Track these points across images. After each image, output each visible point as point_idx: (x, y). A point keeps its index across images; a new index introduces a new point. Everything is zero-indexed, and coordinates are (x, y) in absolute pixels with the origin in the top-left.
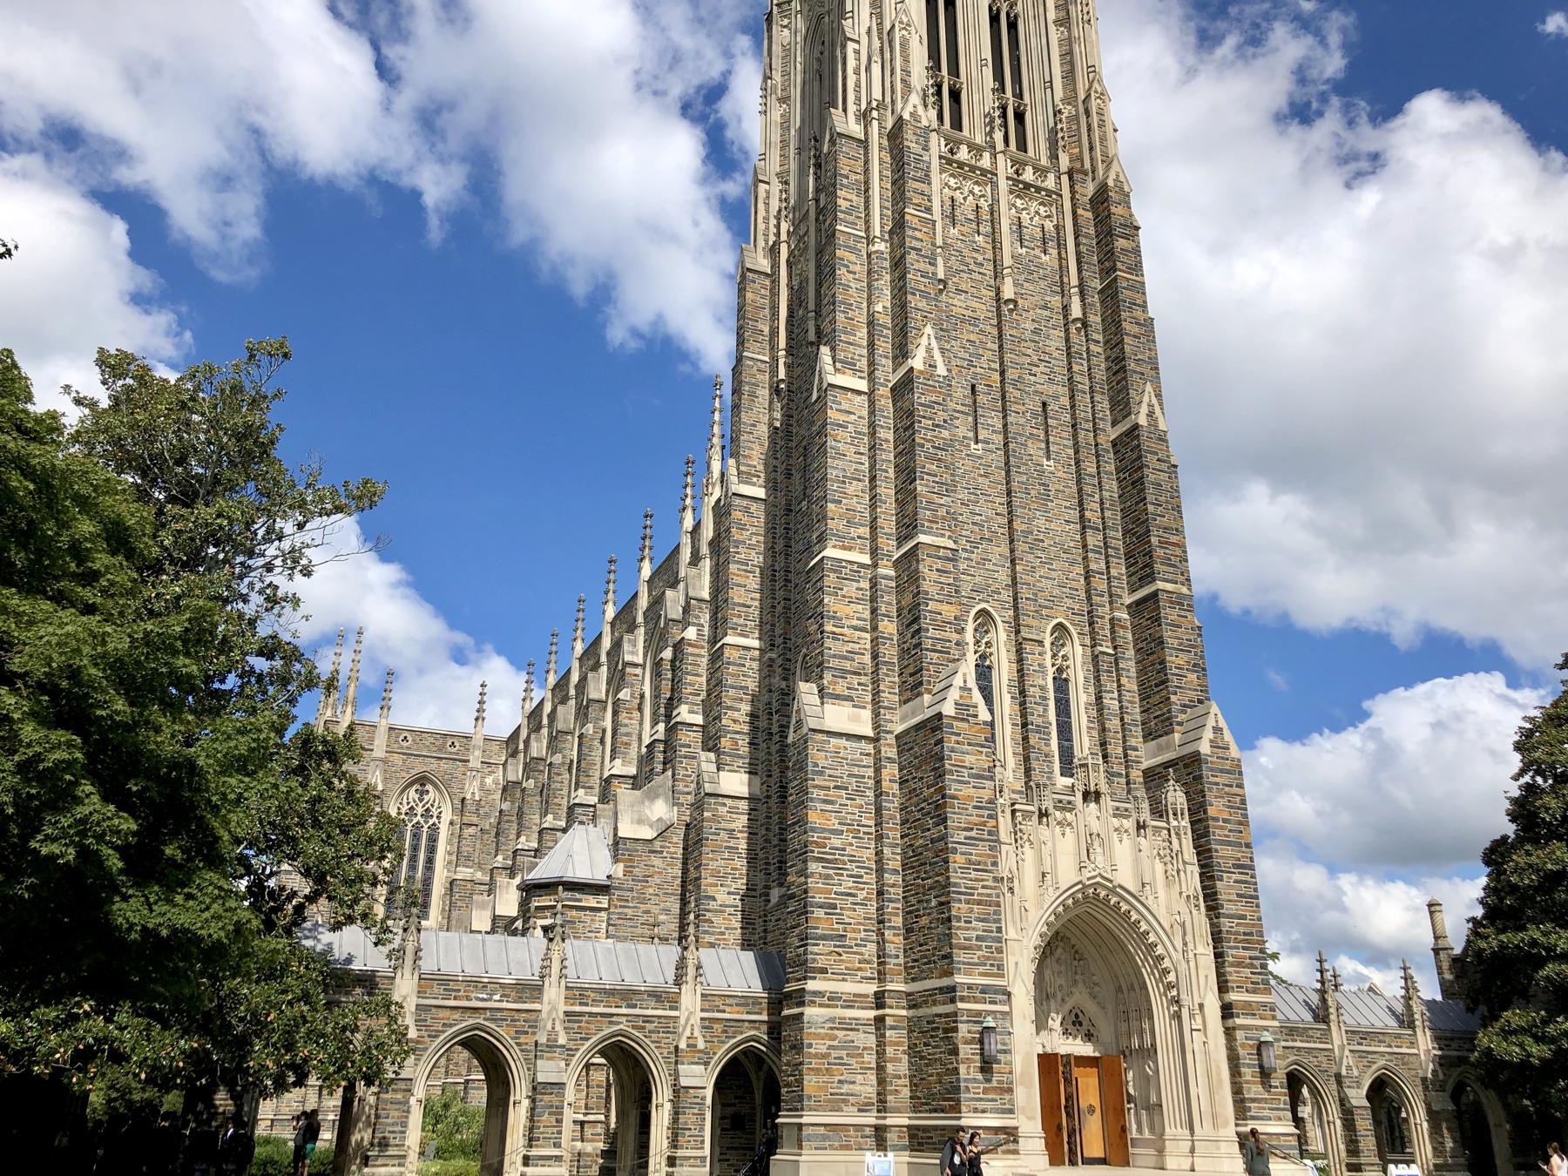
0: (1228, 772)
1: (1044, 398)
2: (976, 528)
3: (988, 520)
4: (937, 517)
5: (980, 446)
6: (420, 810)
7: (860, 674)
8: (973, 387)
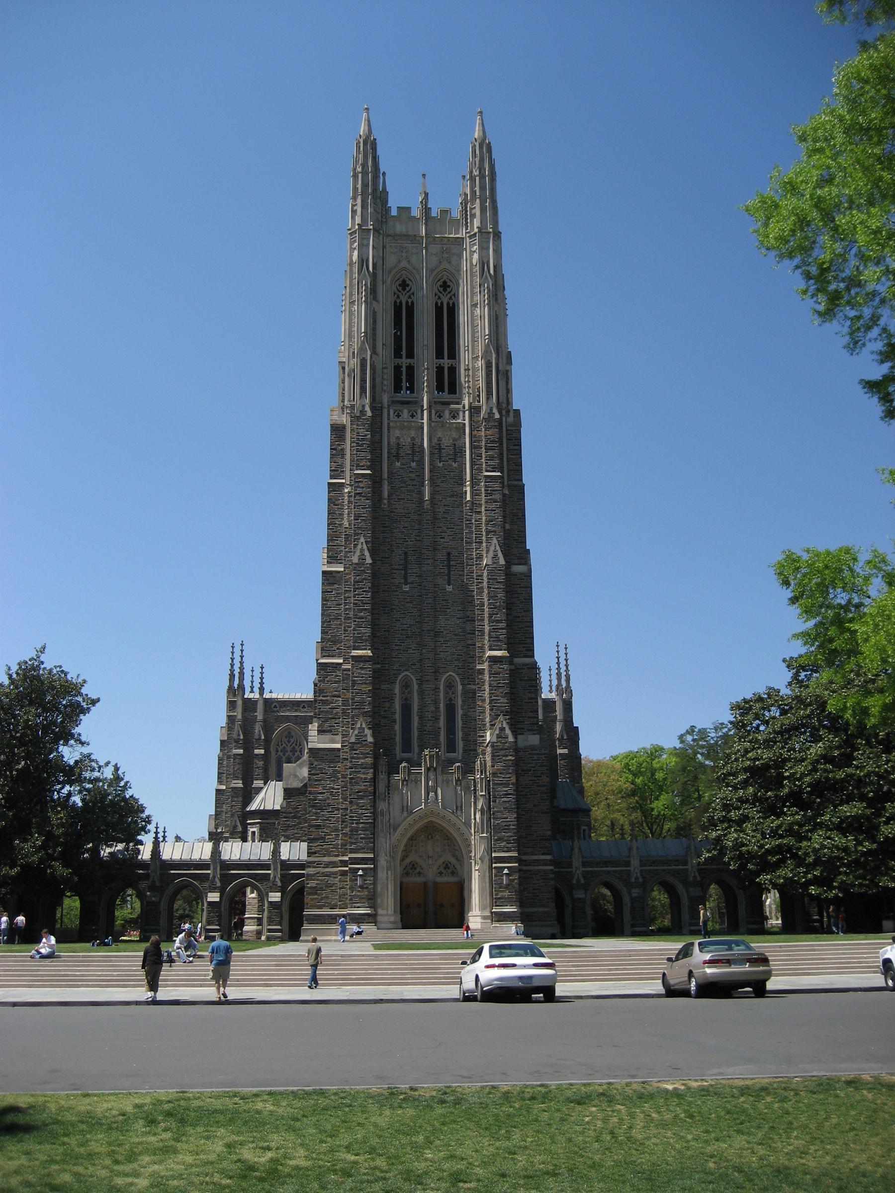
0: (506, 749)
1: (449, 550)
2: (404, 632)
4: (362, 640)
6: (289, 748)
7: (335, 719)
8: (406, 553)
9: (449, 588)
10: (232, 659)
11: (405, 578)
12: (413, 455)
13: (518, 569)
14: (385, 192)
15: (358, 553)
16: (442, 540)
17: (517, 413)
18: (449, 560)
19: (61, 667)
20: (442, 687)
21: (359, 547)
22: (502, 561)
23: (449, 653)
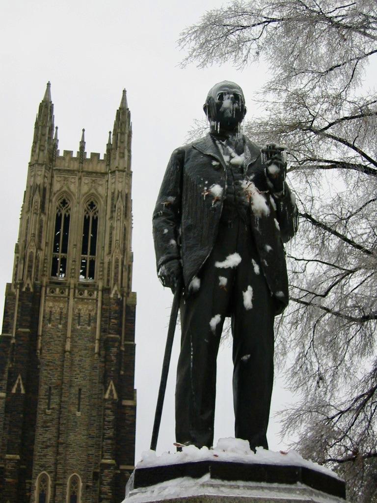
1: (80, 387)
3: (50, 439)
5: (50, 411)
9: (78, 414)
11: (49, 404)
12: (61, 319)
13: (128, 403)
14: (56, 140)
15: (16, 386)
16: (76, 380)
17: (135, 294)
18: (80, 394)
20: (68, 483)
21: (17, 382)
22: (115, 396)
23: (75, 460)
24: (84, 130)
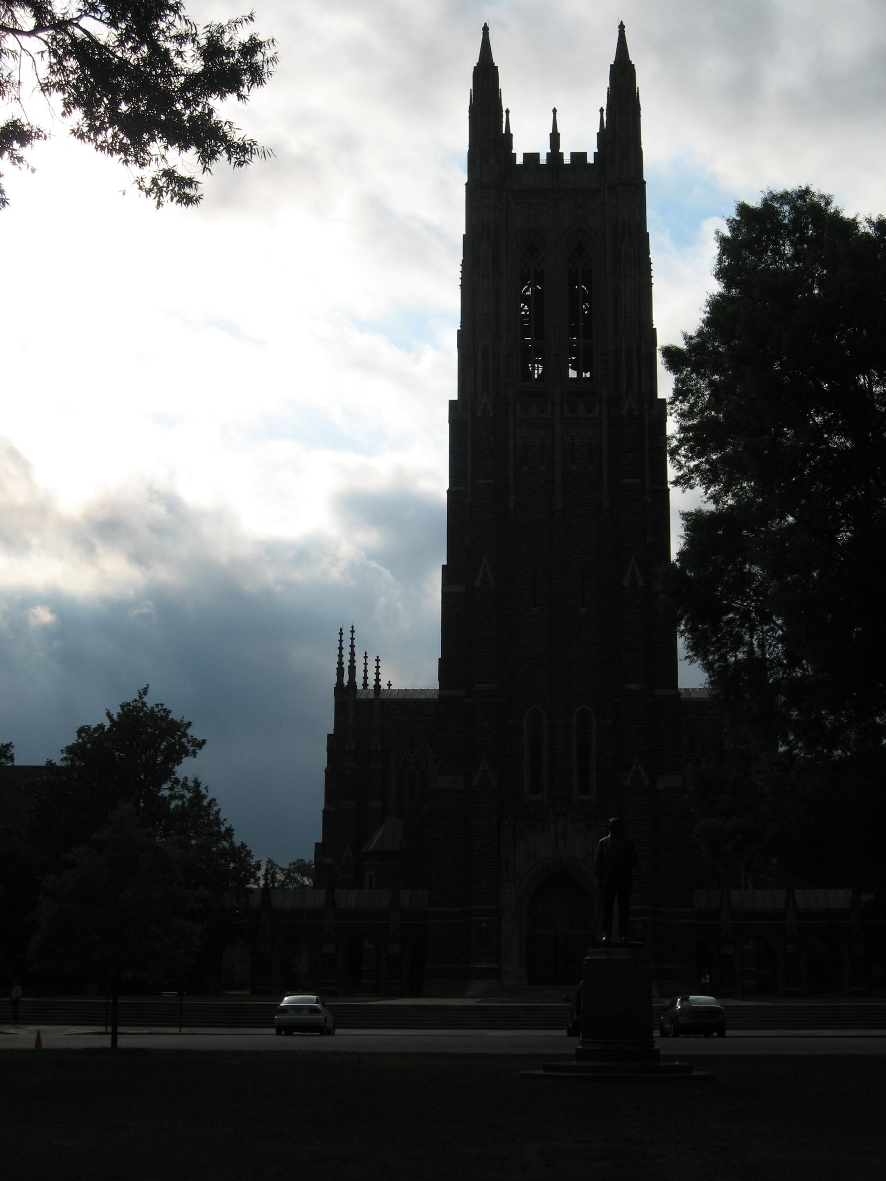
10: (341, 648)
14: (509, 136)
19: (162, 705)
24: (555, 111)
